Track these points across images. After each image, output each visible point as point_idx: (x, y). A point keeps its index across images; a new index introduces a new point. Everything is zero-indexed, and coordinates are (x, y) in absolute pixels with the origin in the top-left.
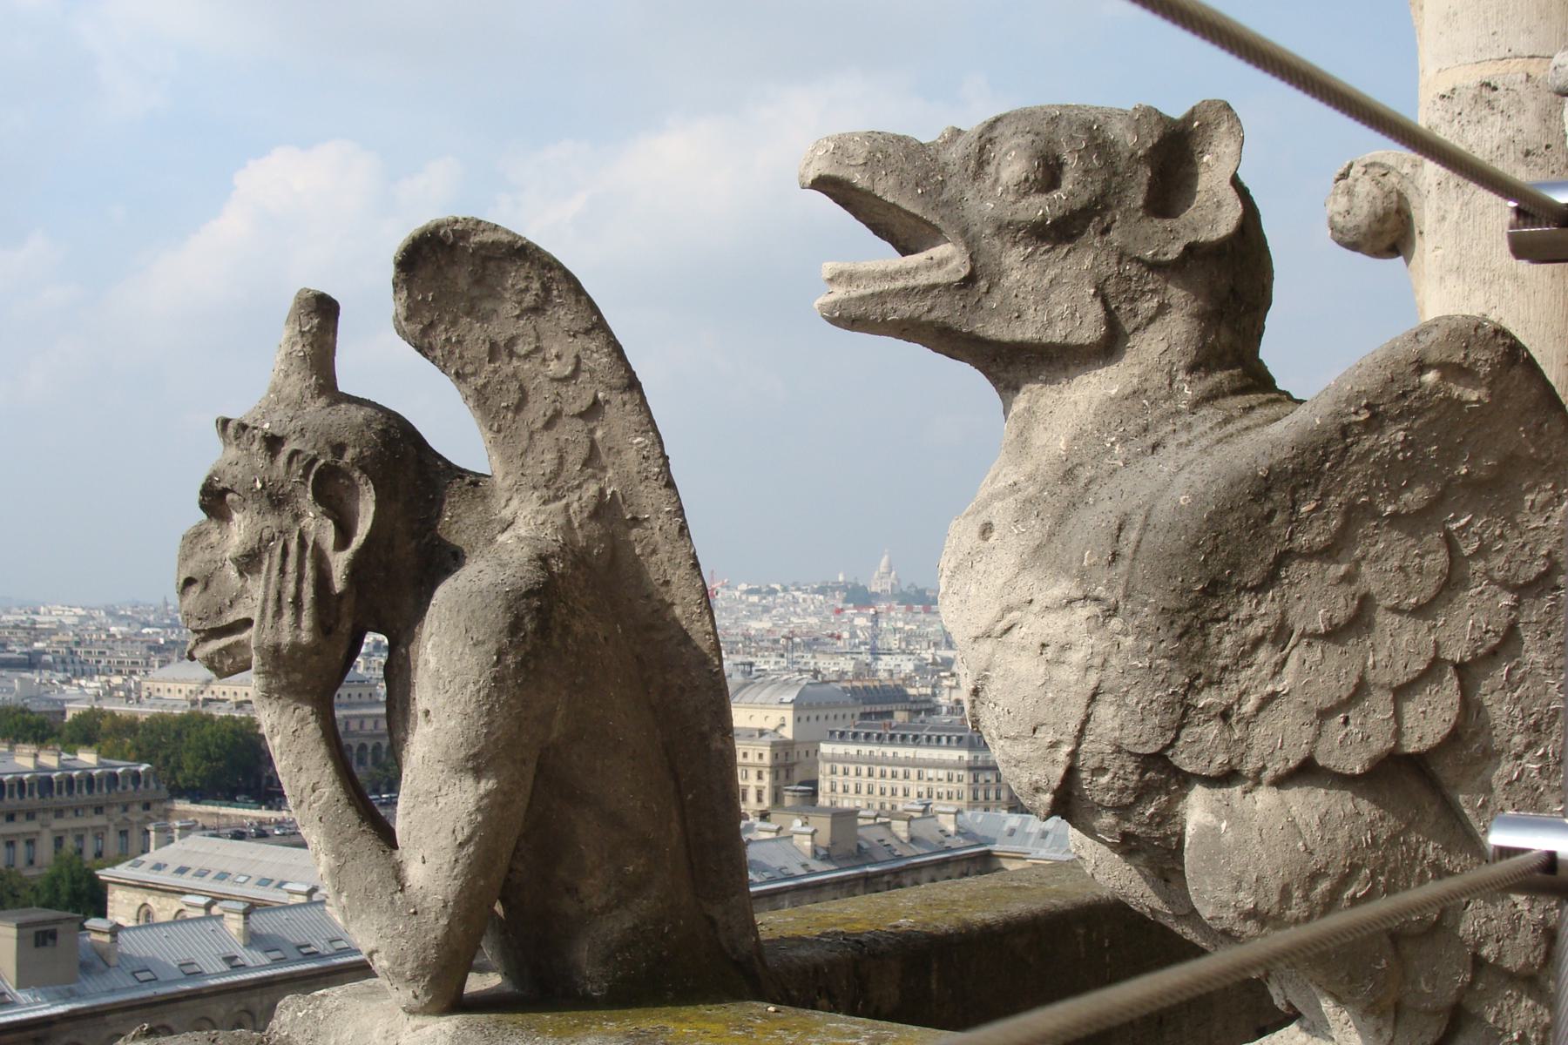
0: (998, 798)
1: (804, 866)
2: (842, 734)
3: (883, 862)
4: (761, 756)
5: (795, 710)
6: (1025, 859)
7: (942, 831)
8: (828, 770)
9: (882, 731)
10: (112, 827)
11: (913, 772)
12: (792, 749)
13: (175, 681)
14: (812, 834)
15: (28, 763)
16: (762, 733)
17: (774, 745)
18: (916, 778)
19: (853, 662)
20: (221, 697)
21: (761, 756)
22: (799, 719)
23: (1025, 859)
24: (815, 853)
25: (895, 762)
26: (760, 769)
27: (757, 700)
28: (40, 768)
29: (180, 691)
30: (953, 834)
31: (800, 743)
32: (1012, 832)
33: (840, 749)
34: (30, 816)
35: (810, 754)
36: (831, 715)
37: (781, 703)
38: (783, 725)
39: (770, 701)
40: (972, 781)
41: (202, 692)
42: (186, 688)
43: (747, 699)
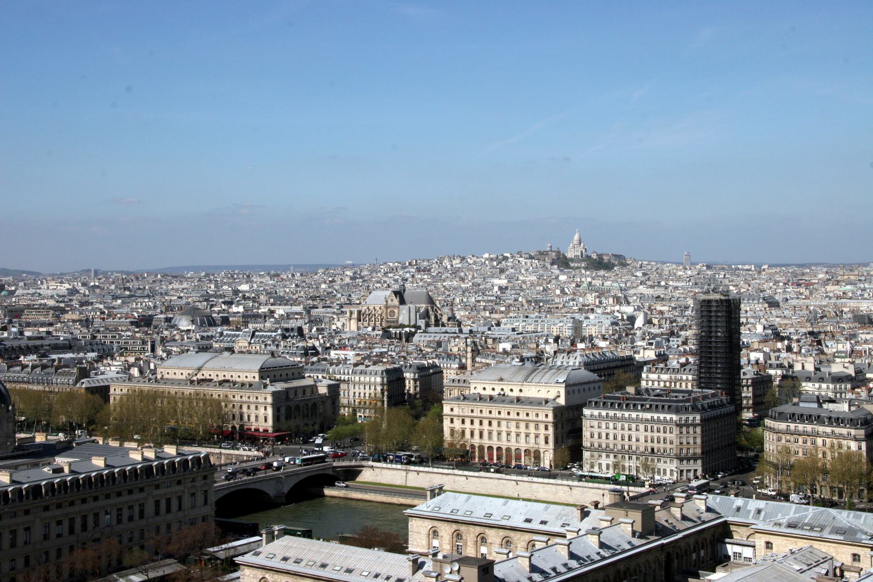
0: (695, 443)
1: (630, 543)
2: (596, 403)
4: (547, 416)
5: (566, 386)
7: (698, 510)
8: (588, 425)
9: (621, 401)
10: (186, 491)
11: (642, 427)
13: (179, 368)
14: (632, 524)
15: (136, 456)
16: (547, 401)
18: (643, 431)
20: (208, 377)
21: (547, 416)
24: (634, 533)
25: (630, 420)
27: (543, 380)
28: (145, 459)
29: (182, 374)
30: (704, 511)
32: (738, 509)
33: (596, 412)
34: (141, 490)
37: (557, 382)
38: (559, 396)
39: (550, 381)
40: (678, 433)
41: (196, 375)
42: (186, 373)
43: (537, 379)
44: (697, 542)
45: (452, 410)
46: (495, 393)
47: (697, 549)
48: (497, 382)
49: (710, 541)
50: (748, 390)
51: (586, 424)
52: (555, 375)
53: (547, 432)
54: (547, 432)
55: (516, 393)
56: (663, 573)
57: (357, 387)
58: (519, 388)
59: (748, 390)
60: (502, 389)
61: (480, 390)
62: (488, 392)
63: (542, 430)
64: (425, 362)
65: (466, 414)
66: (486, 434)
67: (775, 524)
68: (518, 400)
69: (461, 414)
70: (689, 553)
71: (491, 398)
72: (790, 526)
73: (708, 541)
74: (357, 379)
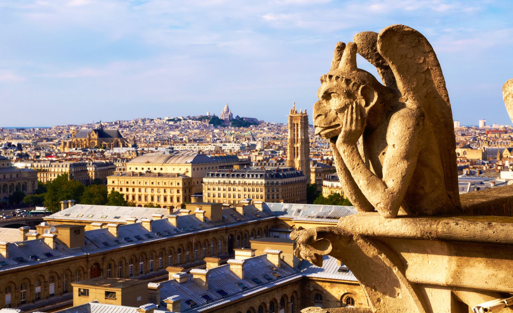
3: (233, 223)
4: (178, 184)
6: (291, 220)
8: (207, 189)
9: (229, 173)
12: (192, 181)
16: (179, 175)
17: (183, 180)
18: (243, 191)
19: (214, 147)
21: (178, 184)
22: (194, 169)
23: (291, 220)
26: (178, 189)
31: (195, 178)
33: (211, 180)
35: (199, 182)
36: (207, 167)
37: (186, 163)
44: (254, 230)
45: (113, 182)
46: (144, 172)
47: (254, 234)
48: (145, 164)
49: (265, 230)
50: (320, 175)
51: (205, 187)
52: (186, 158)
53: (178, 194)
54: (178, 194)
55: (158, 171)
56: (227, 247)
57: (53, 175)
58: (160, 167)
59: (320, 175)
60: (149, 169)
61: (133, 169)
62: (139, 170)
63: (175, 194)
64: (104, 161)
65: (123, 184)
66: (137, 197)
67: (309, 217)
68: (160, 175)
69: (120, 184)
70: (248, 236)
71: (141, 174)
72: (318, 217)
73: (263, 230)
74: (53, 170)
